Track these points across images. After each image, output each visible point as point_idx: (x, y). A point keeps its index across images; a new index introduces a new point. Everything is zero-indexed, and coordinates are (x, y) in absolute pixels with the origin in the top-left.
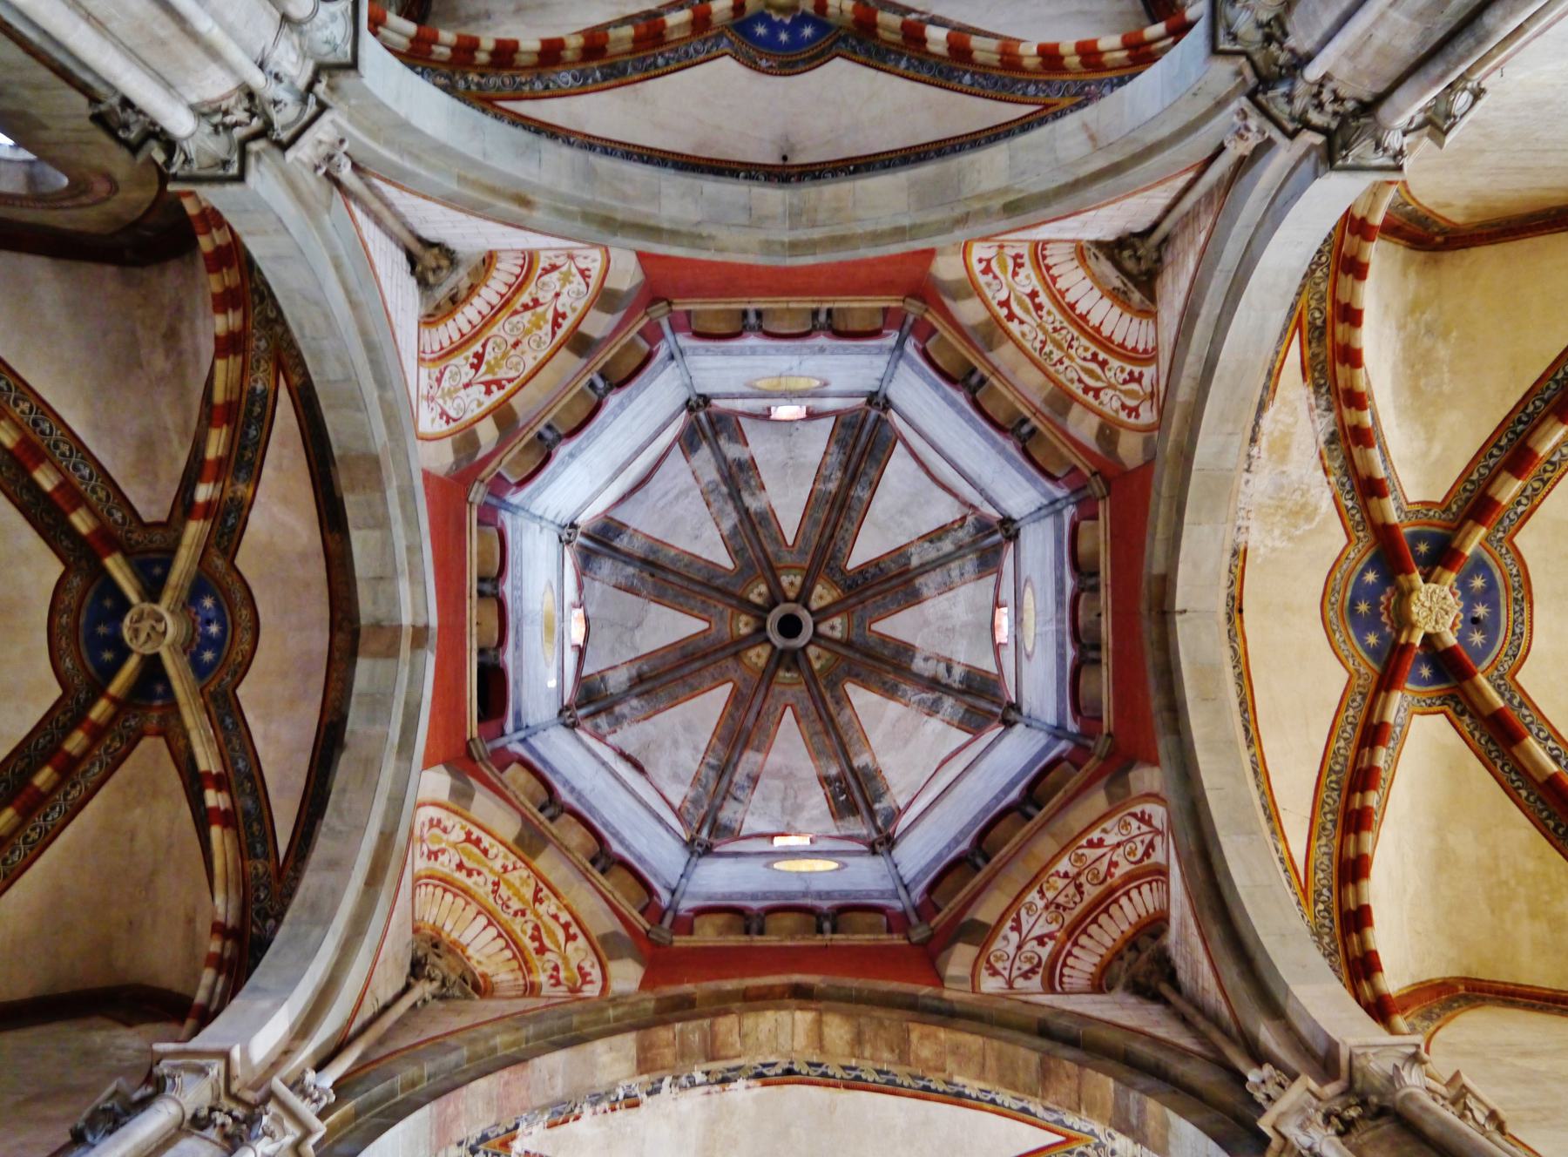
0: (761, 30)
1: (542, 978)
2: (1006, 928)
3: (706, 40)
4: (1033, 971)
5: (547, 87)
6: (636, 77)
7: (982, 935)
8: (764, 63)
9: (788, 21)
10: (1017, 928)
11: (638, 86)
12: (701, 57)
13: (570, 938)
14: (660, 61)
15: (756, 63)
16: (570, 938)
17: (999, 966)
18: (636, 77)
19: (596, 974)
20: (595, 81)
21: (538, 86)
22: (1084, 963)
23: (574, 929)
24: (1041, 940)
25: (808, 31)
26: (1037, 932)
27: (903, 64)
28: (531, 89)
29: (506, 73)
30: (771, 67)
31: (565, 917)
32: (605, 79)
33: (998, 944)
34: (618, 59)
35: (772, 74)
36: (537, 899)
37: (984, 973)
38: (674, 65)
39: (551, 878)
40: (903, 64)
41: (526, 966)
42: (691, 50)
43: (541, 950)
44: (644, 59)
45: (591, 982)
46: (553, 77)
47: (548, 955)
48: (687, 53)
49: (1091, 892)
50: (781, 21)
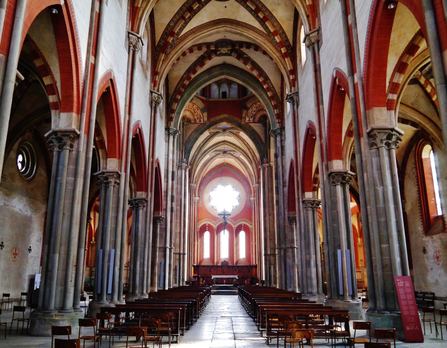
1: (196, 117)
2: (250, 109)
4: (252, 116)
7: (247, 109)
10: (252, 109)
13: (198, 110)
16: (198, 110)
17: (249, 115)
19: (202, 115)
22: (258, 116)
23: (198, 108)
24: (254, 111)
26: (254, 110)
31: (197, 107)
33: (249, 111)
36: (193, 106)
37: (247, 116)
39: (194, 103)
41: (194, 116)
43: (195, 113)
45: (201, 118)
47: (196, 113)
49: (261, 108)
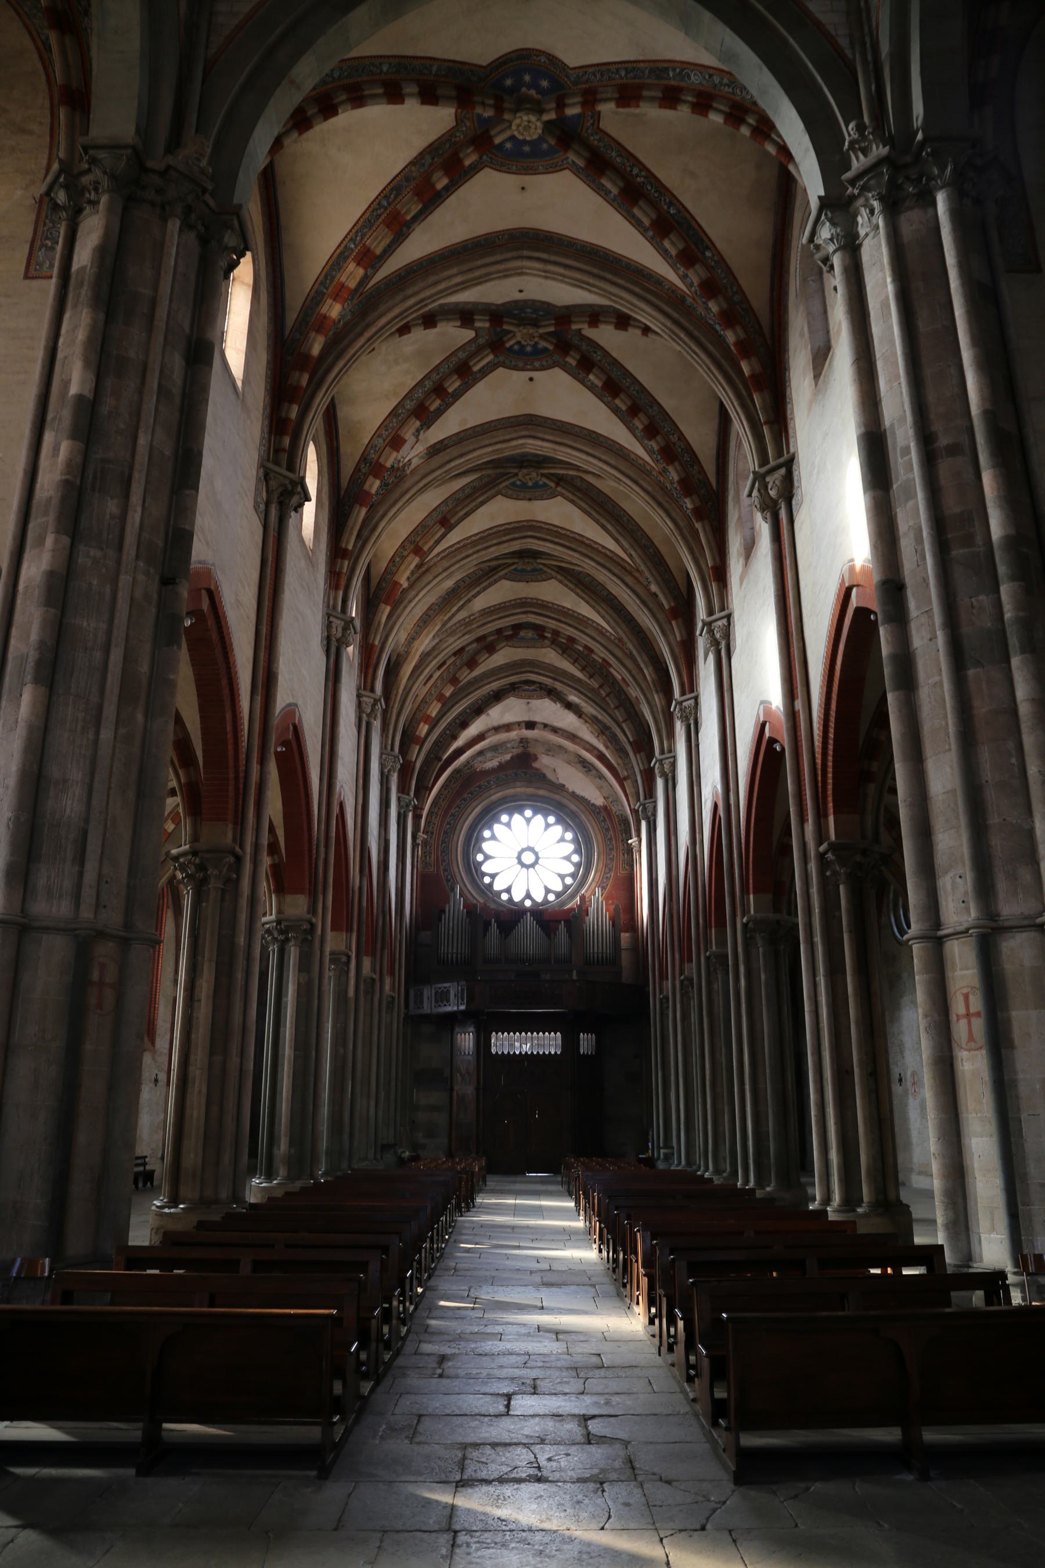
0: (545, 84)
3: (587, 82)
5: (711, 76)
6: (642, 65)
8: (543, 59)
9: (524, 89)
11: (641, 58)
12: (591, 70)
14: (623, 73)
15: (549, 60)
18: (642, 65)
20: (674, 70)
21: (716, 79)
25: (509, 82)
27: (434, 69)
28: (722, 79)
29: (738, 98)
30: (537, 56)
32: (667, 69)
34: (656, 82)
35: (537, 50)
38: (613, 68)
40: (434, 69)
42: (598, 76)
44: (634, 78)
46: (704, 82)
48: (602, 75)
50: (529, 90)
